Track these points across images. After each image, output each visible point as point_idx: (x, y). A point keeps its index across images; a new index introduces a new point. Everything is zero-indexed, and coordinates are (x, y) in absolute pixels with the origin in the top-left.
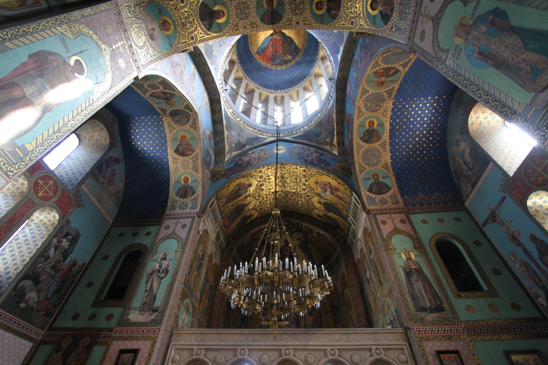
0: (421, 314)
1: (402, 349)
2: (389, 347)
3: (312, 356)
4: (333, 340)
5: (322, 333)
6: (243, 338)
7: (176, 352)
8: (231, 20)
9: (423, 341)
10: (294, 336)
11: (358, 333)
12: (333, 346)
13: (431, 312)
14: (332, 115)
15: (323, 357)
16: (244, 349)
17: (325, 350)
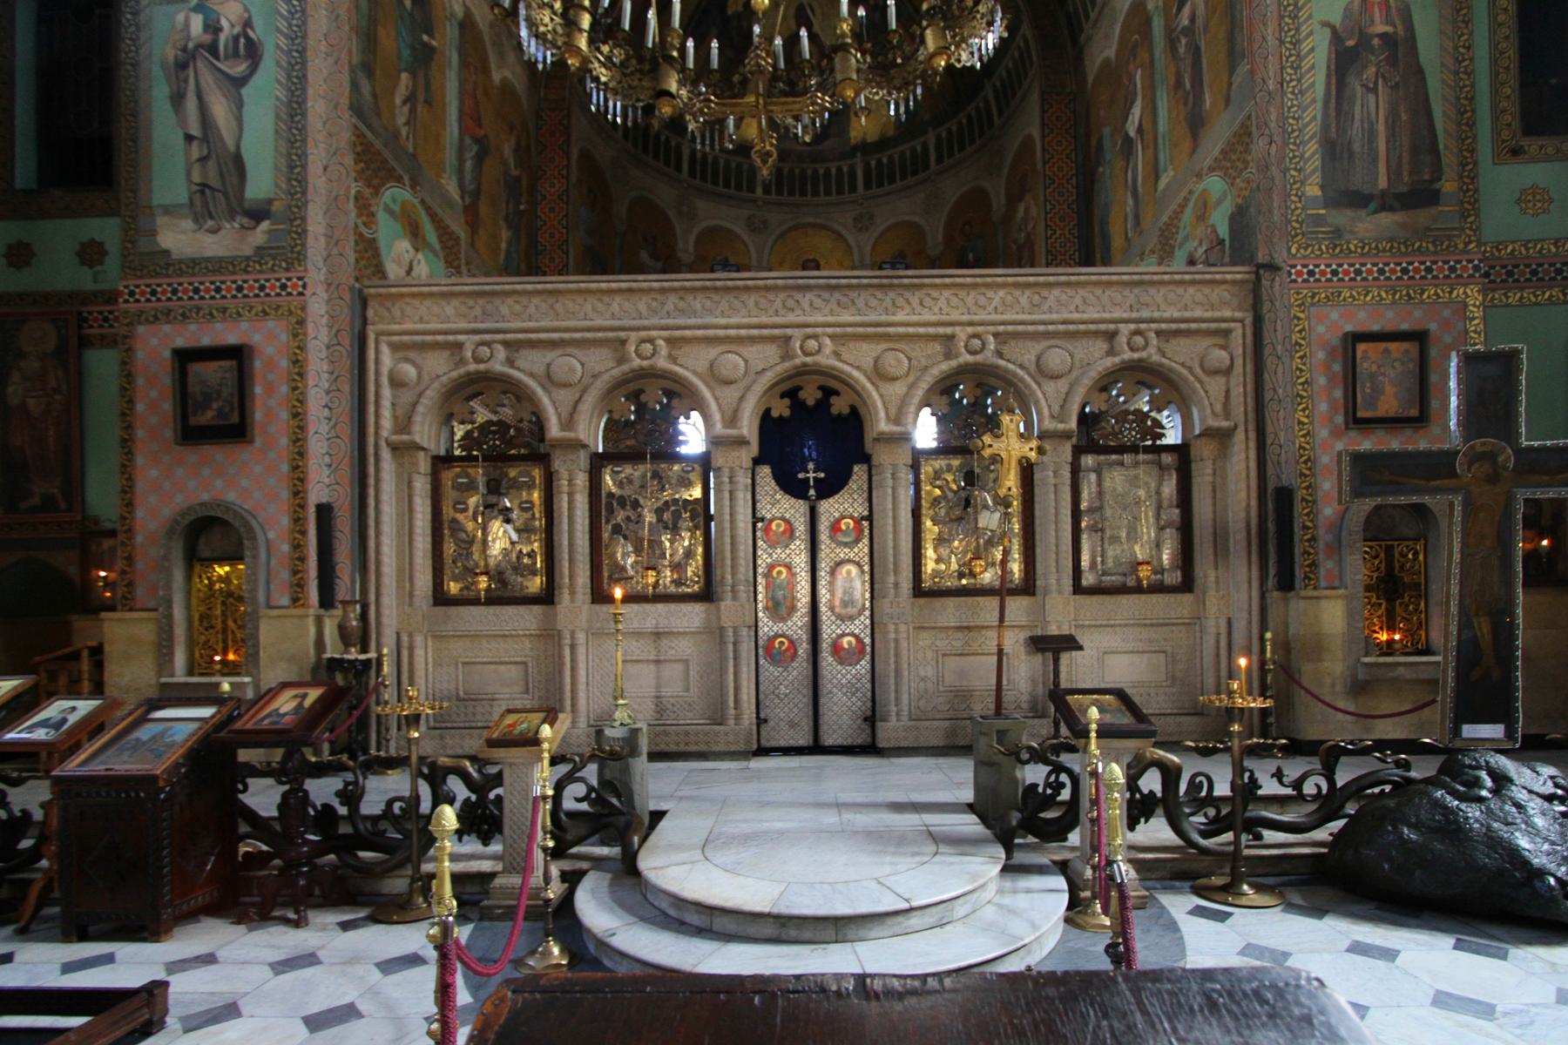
0: (1341, 218)
1: (1226, 333)
3: (902, 356)
4: (984, 308)
5: (946, 286)
6: (642, 306)
7: (400, 355)
9: (1313, 305)
10: (837, 295)
11: (1078, 284)
12: (981, 324)
13: (1384, 207)
15: (941, 358)
16: (651, 341)
17: (952, 337)
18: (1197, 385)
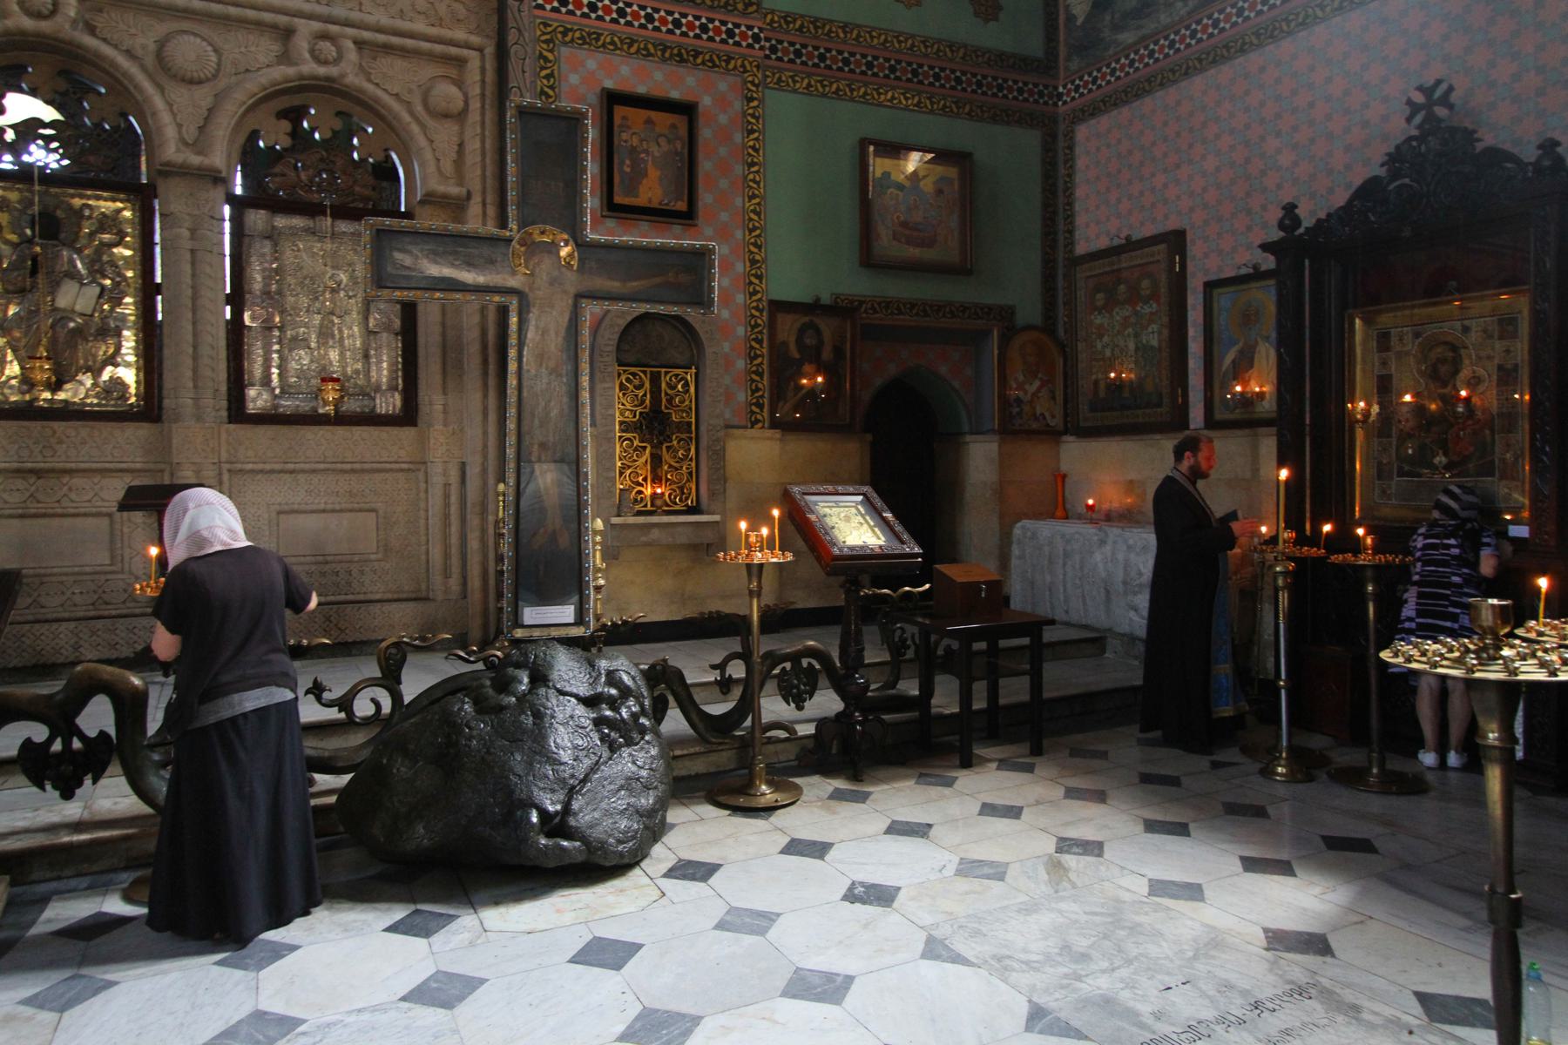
1: (461, 62)
2: (395, 40)
9: (565, 44)
18: (415, 128)
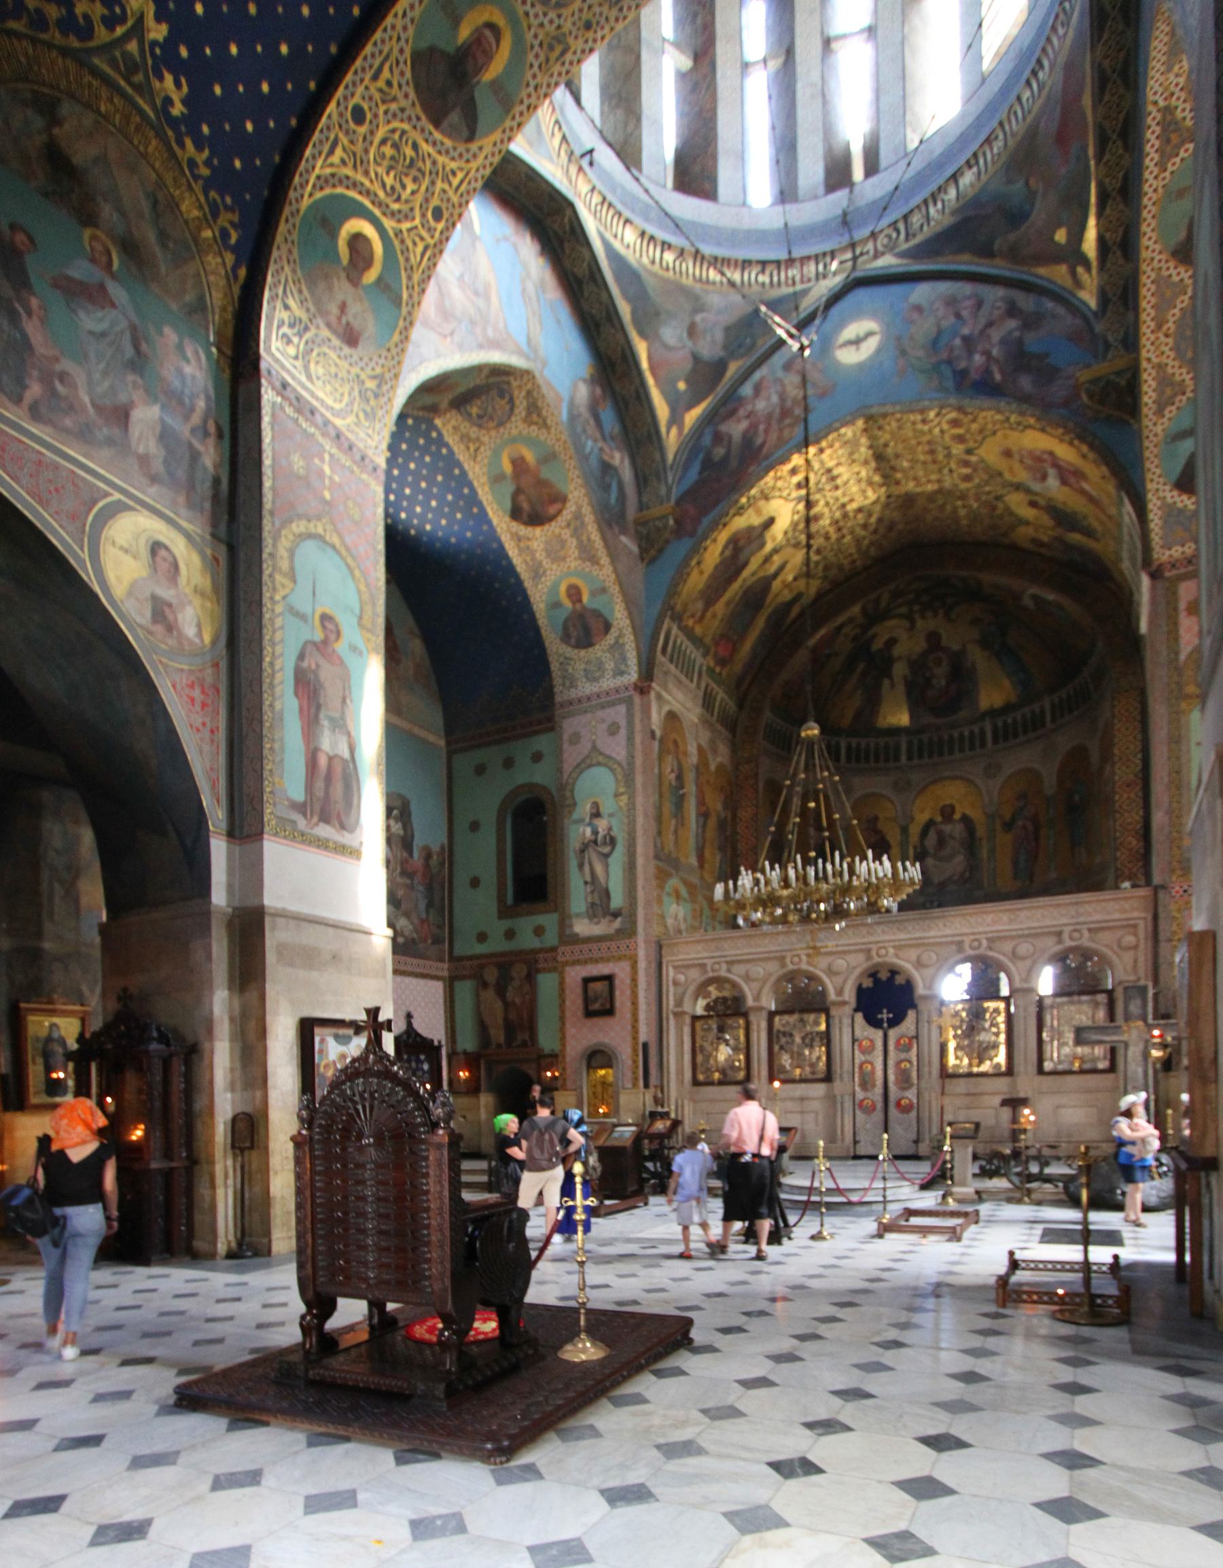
8: (529, 36)
14: (1078, 97)
